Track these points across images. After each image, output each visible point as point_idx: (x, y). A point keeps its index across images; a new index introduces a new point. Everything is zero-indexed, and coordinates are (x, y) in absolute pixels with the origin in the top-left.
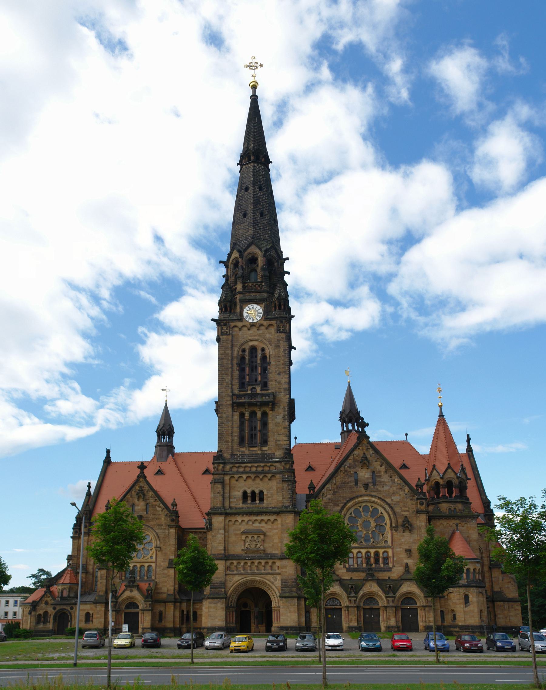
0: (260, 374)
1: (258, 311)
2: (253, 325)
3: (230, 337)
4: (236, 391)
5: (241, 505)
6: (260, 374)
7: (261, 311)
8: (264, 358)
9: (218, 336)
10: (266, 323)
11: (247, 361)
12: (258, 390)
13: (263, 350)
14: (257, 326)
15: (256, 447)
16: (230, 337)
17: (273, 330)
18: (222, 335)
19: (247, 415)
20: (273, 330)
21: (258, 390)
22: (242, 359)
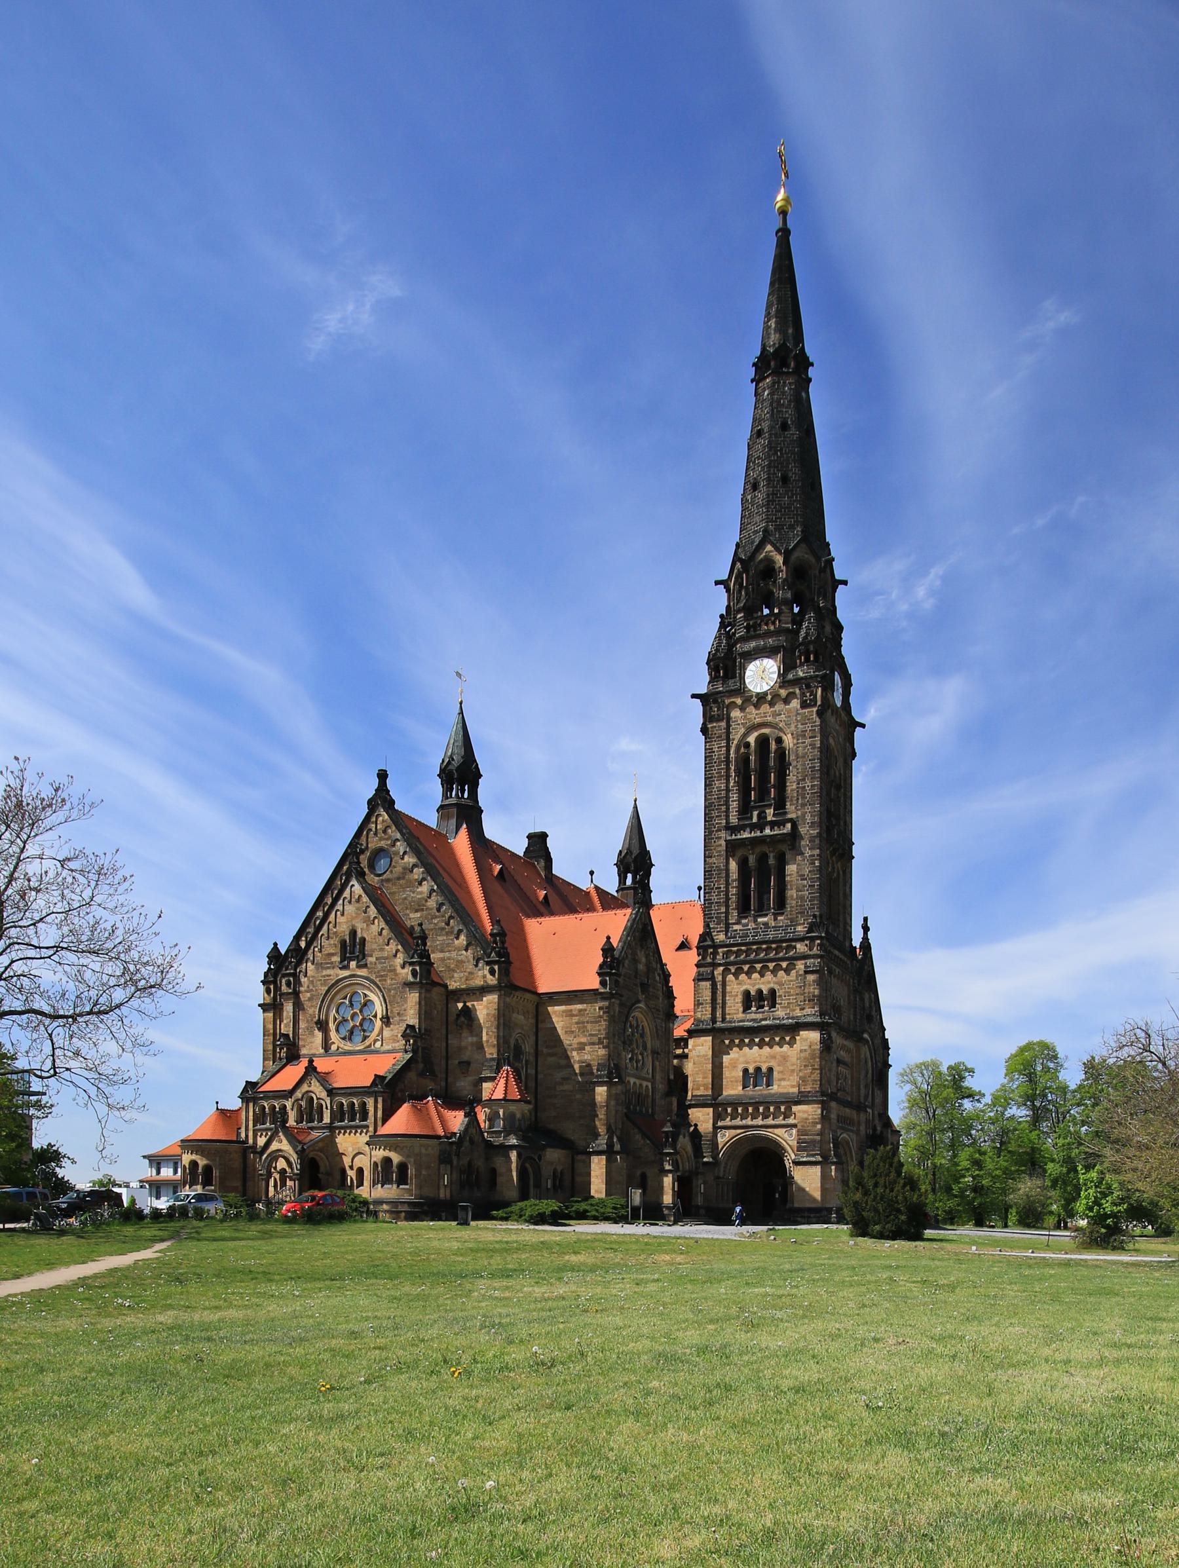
0: (774, 786)
1: (771, 670)
2: (761, 697)
3: (723, 724)
4: (734, 820)
5: (741, 1016)
6: (774, 786)
7: (775, 669)
8: (782, 754)
9: (704, 724)
10: (783, 693)
11: (752, 765)
12: (770, 813)
13: (779, 741)
14: (769, 697)
15: (766, 915)
16: (723, 724)
17: (795, 703)
18: (711, 721)
19: (752, 860)
20: (795, 703)
21: (770, 813)
22: (745, 759)
